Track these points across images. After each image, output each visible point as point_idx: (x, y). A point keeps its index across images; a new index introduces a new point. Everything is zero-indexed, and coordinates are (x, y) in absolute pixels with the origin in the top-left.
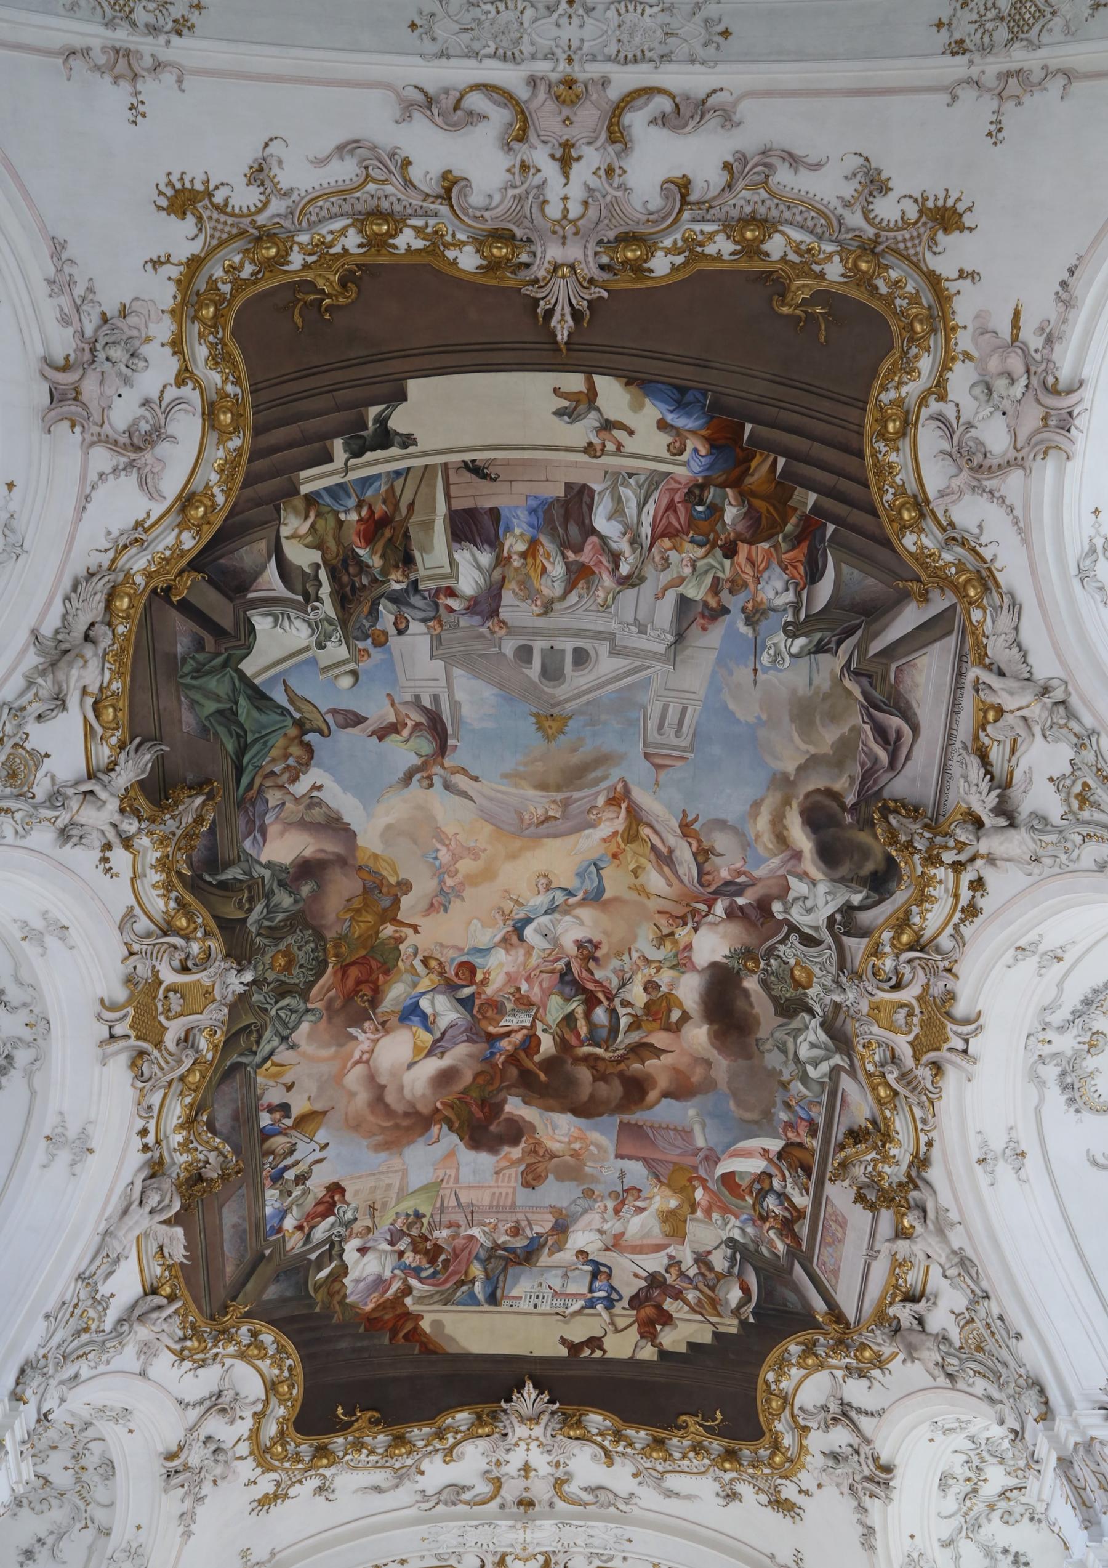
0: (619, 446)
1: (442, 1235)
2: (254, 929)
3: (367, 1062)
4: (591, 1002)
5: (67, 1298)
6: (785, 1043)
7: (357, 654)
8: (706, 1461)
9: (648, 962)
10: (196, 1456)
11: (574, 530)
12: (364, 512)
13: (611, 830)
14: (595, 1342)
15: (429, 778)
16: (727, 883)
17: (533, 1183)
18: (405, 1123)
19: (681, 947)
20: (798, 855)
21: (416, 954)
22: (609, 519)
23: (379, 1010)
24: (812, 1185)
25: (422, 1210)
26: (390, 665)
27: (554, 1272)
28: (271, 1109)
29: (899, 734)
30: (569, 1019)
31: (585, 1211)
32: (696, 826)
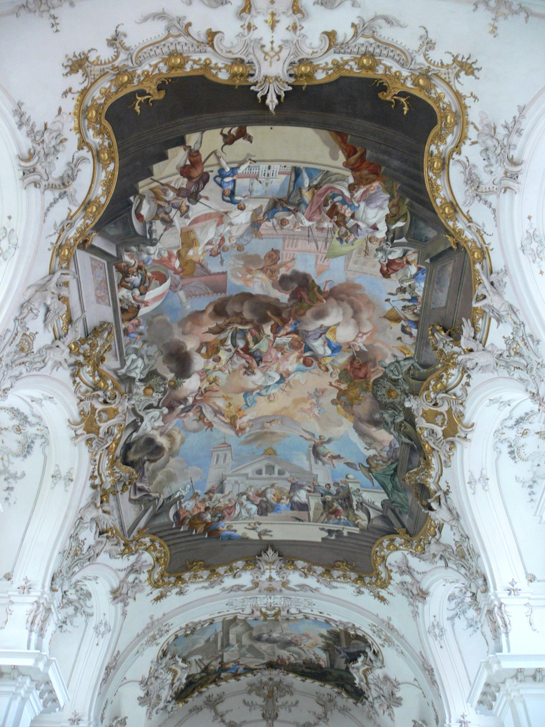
0: (249, 524)
1: (327, 224)
2: (402, 414)
3: (360, 332)
4: (246, 349)
6: (149, 360)
7: (346, 483)
9: (220, 370)
11: (264, 505)
12: (338, 517)
13: (242, 419)
14: (229, 140)
15: (320, 439)
16: (189, 411)
17: (273, 253)
18: (343, 296)
19: (205, 380)
20: (161, 434)
21: (331, 374)
22: (251, 509)
23: (352, 354)
24: (119, 305)
25: (338, 243)
26: (333, 476)
27: (259, 194)
28: (411, 335)
29: (135, 494)
30: (256, 341)
31: (241, 236)
32: (206, 427)
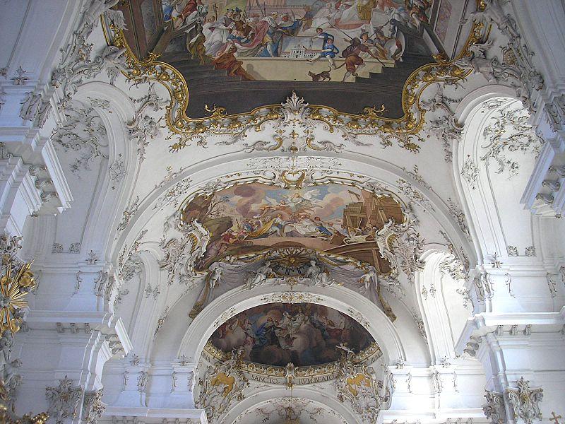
5: (70, 42)
8: (377, 128)
10: (141, 124)
14: (325, 74)
